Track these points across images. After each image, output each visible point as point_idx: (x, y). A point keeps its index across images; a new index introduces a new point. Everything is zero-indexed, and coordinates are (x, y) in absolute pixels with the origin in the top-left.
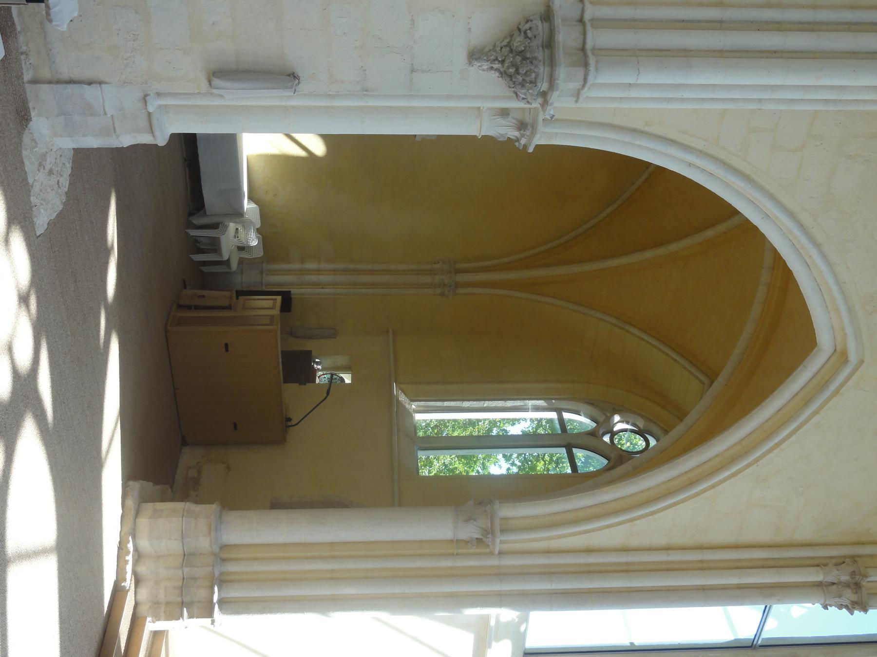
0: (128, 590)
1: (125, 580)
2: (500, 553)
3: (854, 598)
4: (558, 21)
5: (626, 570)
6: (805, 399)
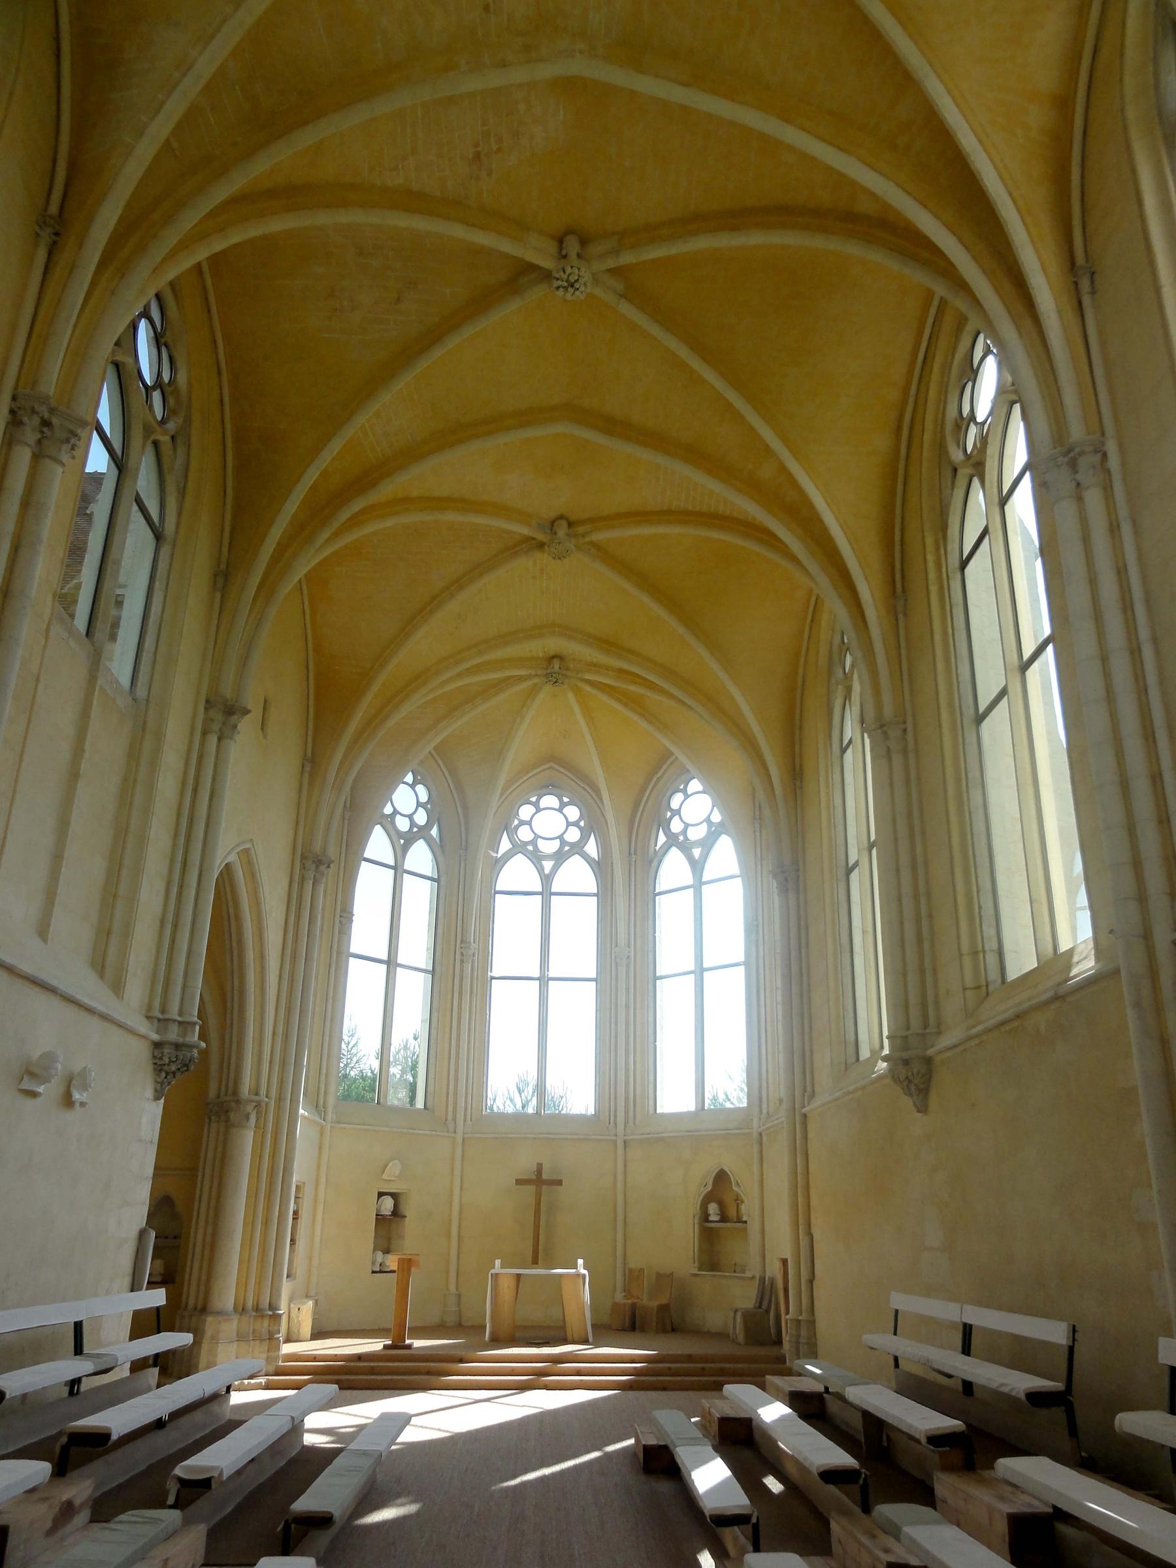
4: (181, 1040)
5: (289, 1010)
6: (252, 875)
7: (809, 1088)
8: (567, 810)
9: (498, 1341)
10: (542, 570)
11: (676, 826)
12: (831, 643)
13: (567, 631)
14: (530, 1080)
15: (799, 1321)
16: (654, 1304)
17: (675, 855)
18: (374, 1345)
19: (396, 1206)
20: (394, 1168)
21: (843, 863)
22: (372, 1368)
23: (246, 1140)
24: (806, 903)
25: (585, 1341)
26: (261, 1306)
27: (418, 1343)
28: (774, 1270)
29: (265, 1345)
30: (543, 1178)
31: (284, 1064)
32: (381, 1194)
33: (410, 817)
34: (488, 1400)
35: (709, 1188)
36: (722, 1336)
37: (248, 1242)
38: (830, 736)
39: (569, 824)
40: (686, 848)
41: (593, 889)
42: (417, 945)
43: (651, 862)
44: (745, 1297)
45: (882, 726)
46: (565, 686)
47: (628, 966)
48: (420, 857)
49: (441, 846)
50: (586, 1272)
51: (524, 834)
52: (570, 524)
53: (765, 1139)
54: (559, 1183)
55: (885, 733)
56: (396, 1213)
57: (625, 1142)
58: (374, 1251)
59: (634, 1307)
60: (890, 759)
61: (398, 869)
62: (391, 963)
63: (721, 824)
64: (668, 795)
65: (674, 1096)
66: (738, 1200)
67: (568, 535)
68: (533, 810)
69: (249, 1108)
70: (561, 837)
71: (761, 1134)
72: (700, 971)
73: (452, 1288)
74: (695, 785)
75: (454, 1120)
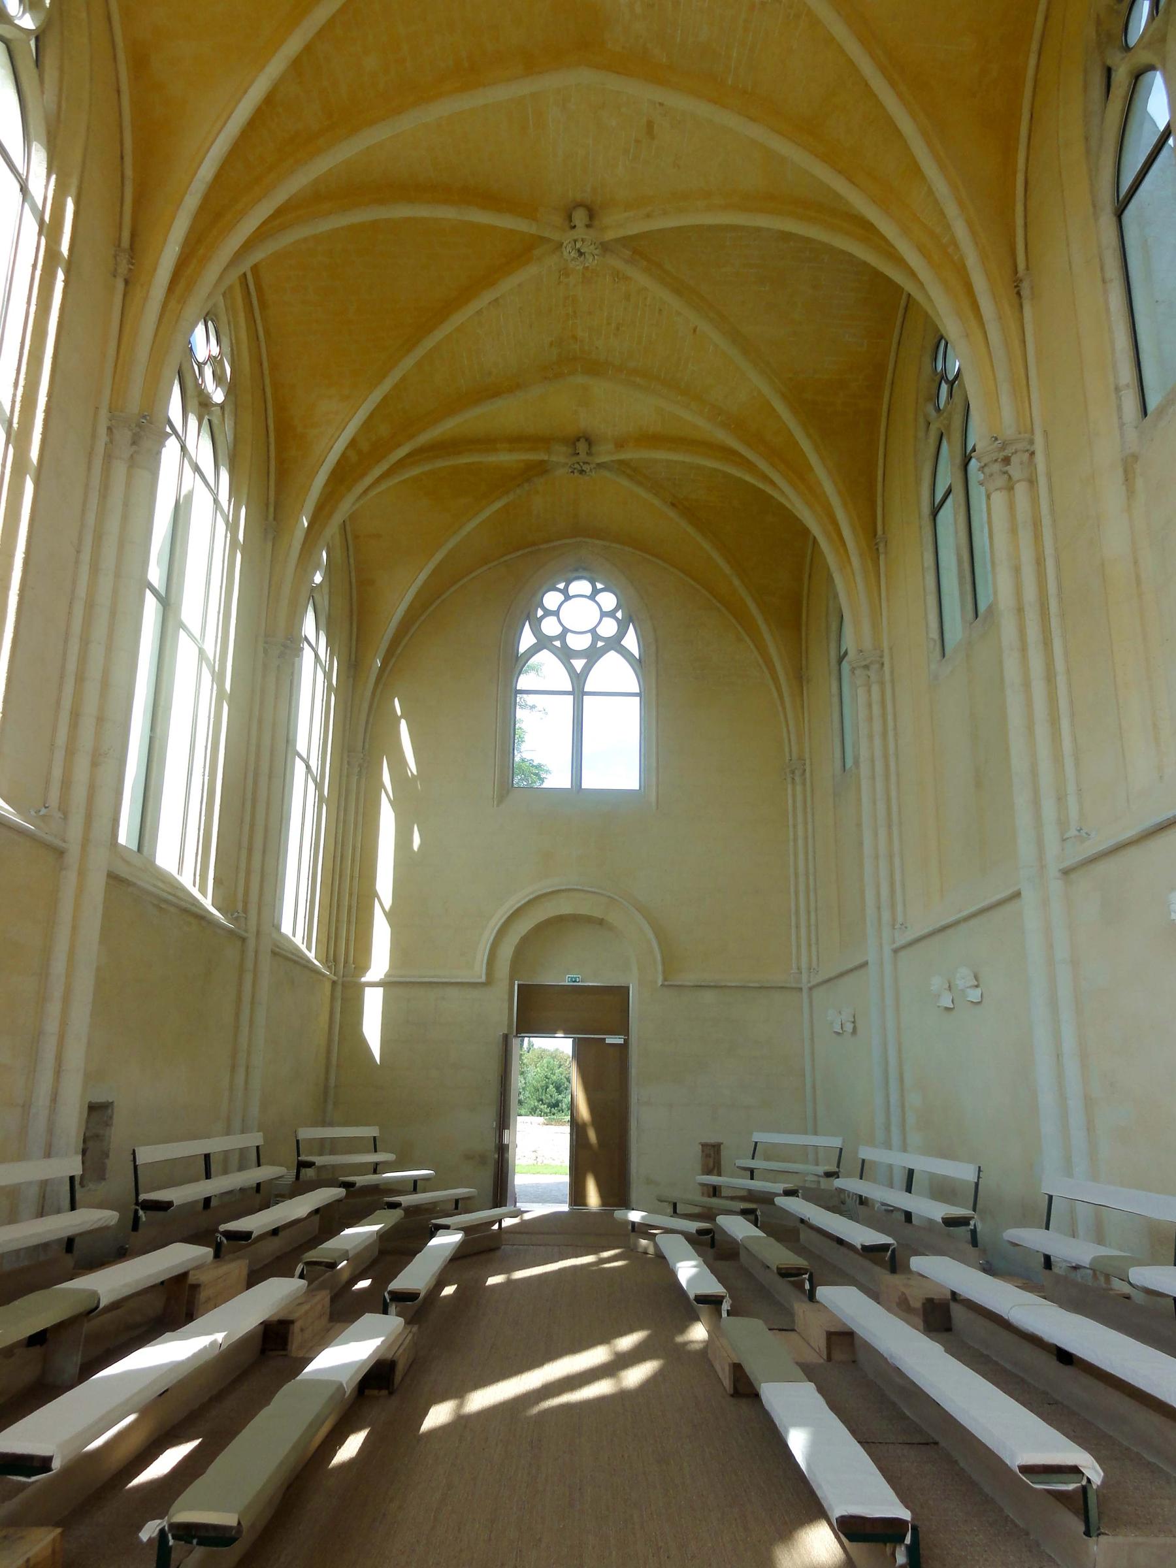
39: (604, 614)
51: (550, 627)
68: (561, 597)
70: (593, 631)
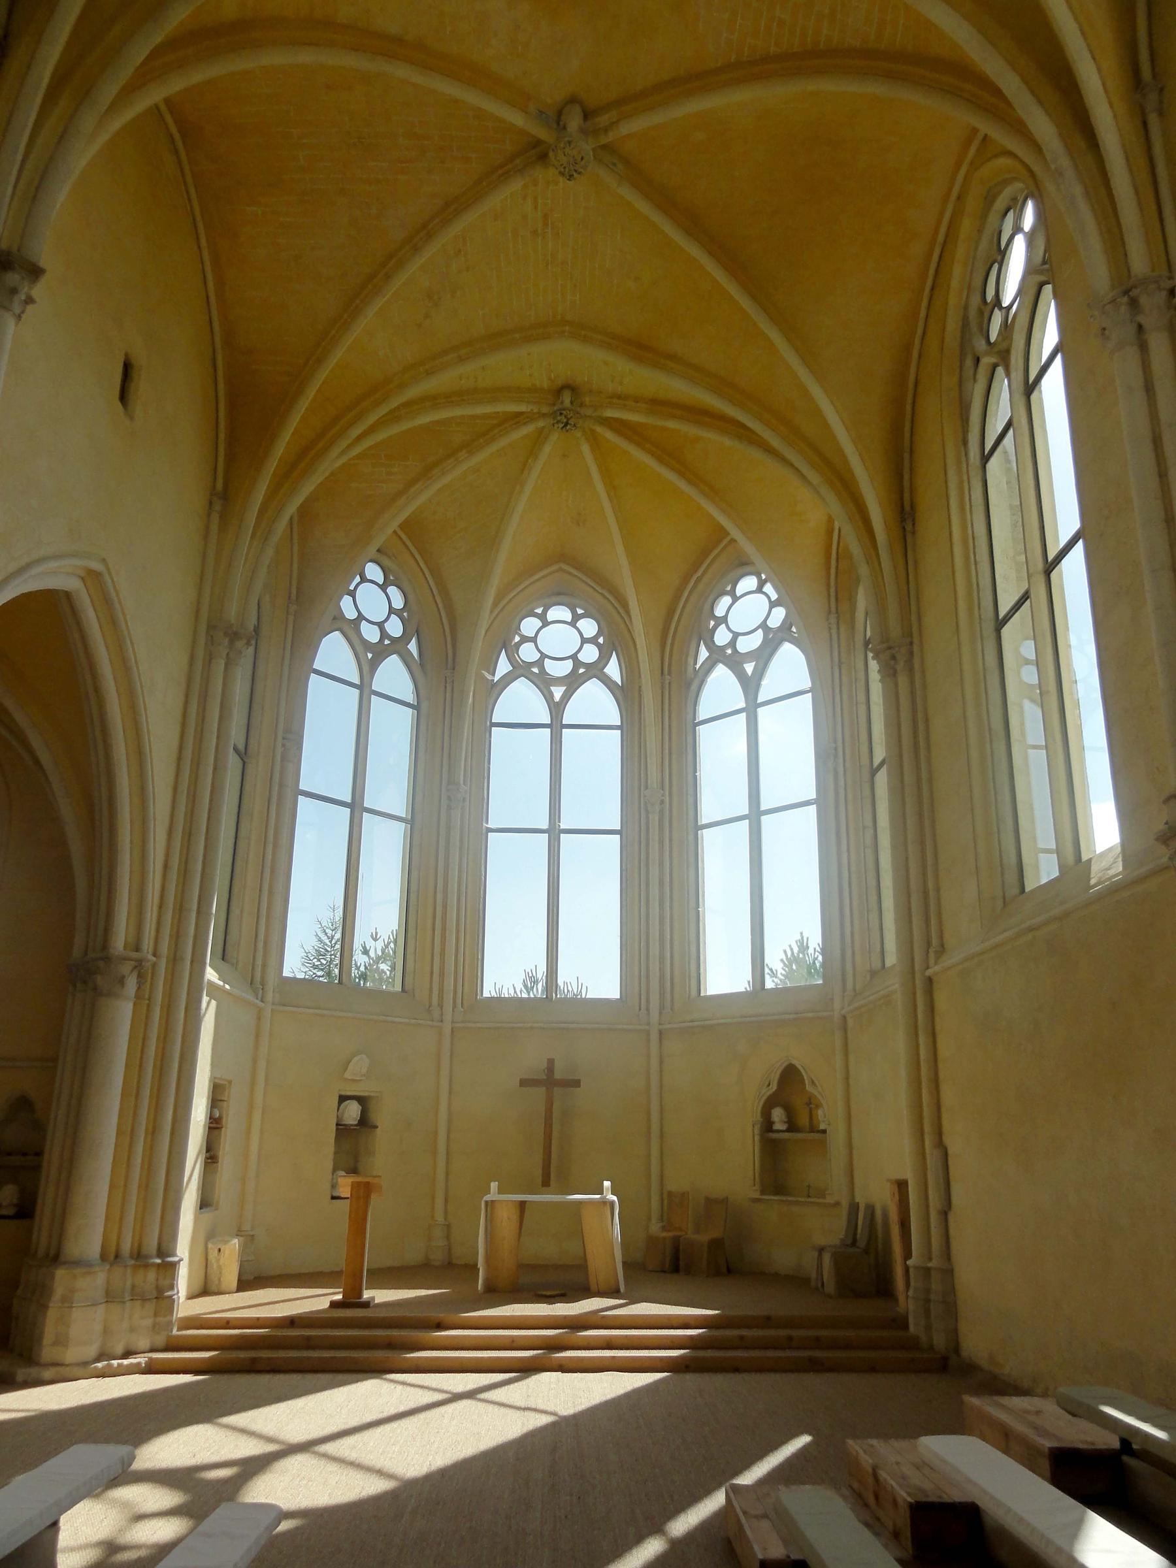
0: (150, 1359)
1: (139, 1364)
2: (154, 955)
3: (245, 641)
5: (189, 835)
6: (112, 622)
7: (935, 941)
8: (581, 624)
9: (498, 1293)
10: (545, 217)
11: (722, 637)
12: (966, 308)
13: (582, 330)
14: (539, 976)
15: (928, 1271)
16: (704, 1238)
17: (721, 671)
18: (315, 1301)
19: (364, 1113)
20: (360, 1065)
21: (991, 614)
22: (309, 1338)
23: (121, 1016)
24: (924, 686)
25: (614, 1293)
26: (144, 1252)
27: (381, 1296)
28: (877, 1193)
29: (150, 1307)
30: (554, 1078)
31: (181, 909)
32: (343, 1099)
33: (381, 625)
34: (471, 1395)
35: (774, 1087)
36: (797, 1281)
37: (122, 1160)
38: (965, 443)
39: (584, 641)
40: (735, 661)
41: (617, 721)
42: (390, 787)
43: (689, 685)
44: (825, 1229)
45: (1126, 292)
46: (578, 434)
47: (662, 812)
48: (394, 676)
49: (422, 665)
50: (615, 1198)
51: (528, 653)
52: (587, 115)
53: (850, 1022)
54: (577, 1083)
55: (1134, 303)
56: (364, 1121)
57: (660, 1033)
58: (335, 1170)
59: (676, 1241)
60: (1143, 347)
61: (364, 689)
62: (356, 807)
63: (786, 626)
64: (712, 597)
65: (724, 973)
66: (812, 1104)
67: (583, 131)
68: (539, 623)
69: (126, 968)
70: (574, 657)
71: (844, 1017)
72: (755, 815)
73: (440, 1217)
74: (748, 583)
75: (441, 1006)
